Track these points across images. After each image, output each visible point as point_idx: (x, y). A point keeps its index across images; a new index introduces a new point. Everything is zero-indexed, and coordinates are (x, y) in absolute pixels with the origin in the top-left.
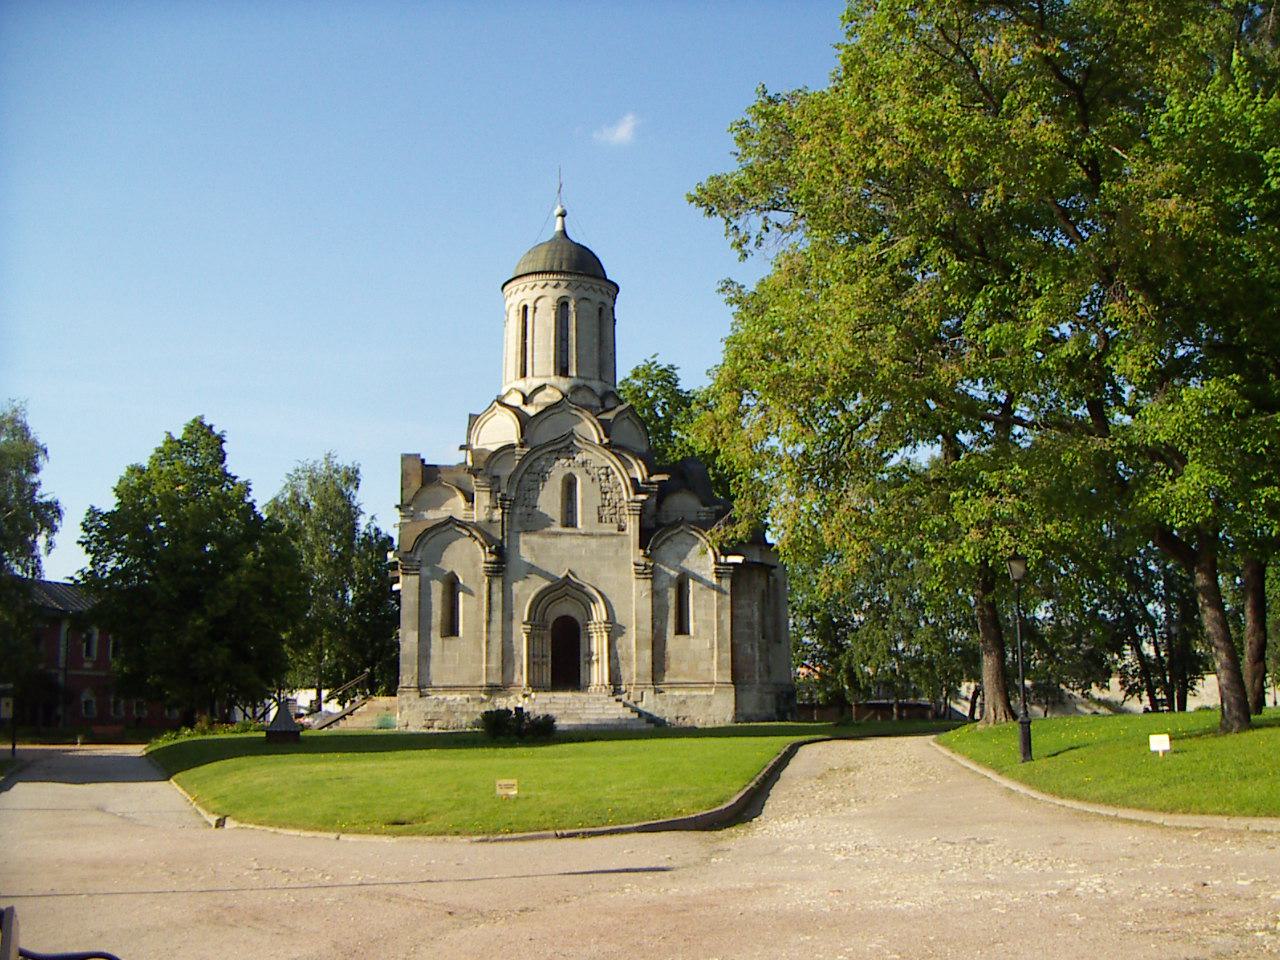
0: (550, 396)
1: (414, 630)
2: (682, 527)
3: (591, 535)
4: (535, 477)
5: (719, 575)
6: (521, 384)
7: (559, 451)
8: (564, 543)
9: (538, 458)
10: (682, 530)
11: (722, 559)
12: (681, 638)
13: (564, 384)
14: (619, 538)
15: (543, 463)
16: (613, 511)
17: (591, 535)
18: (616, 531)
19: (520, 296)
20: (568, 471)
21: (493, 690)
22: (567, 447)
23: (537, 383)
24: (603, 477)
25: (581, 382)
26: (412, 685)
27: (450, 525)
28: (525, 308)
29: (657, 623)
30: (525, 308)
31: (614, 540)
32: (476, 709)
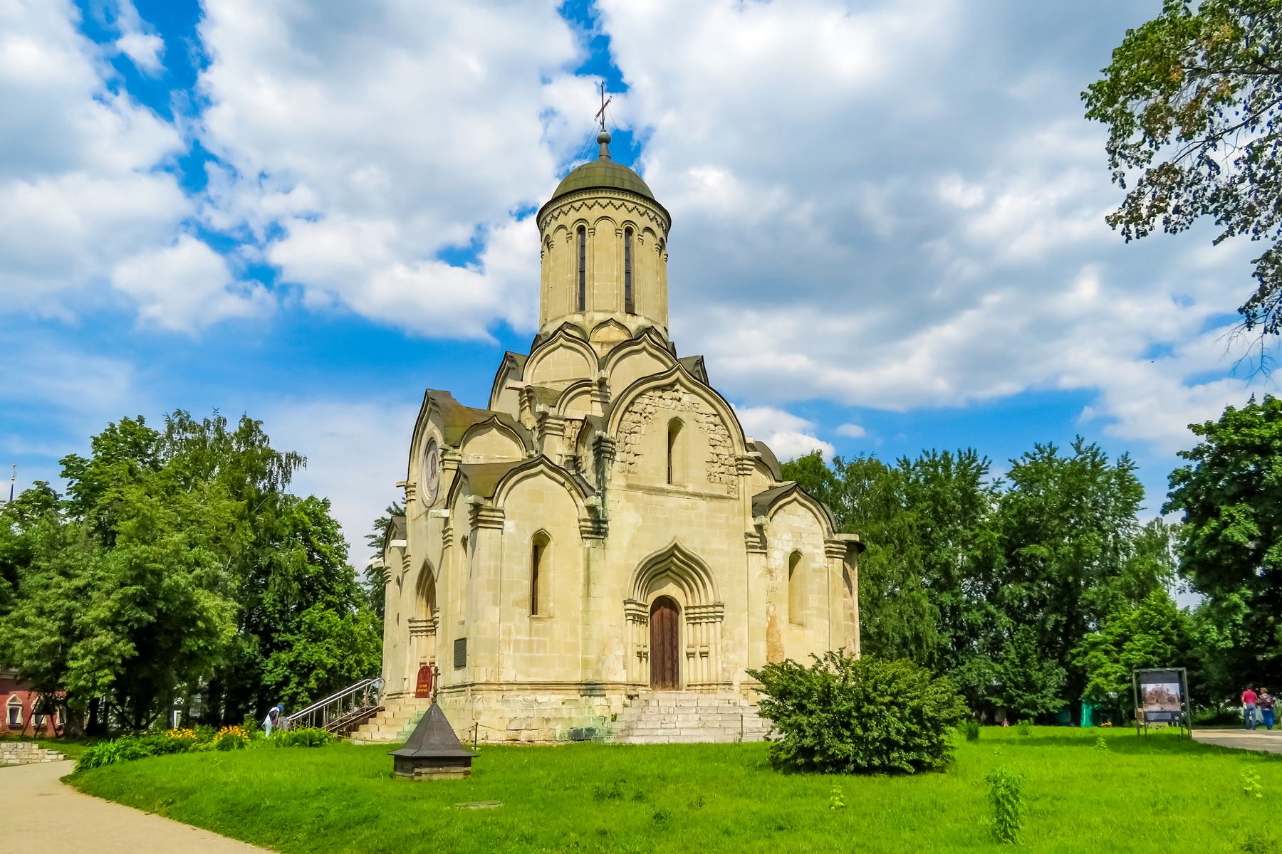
0: (618, 335)
1: (495, 604)
2: (795, 495)
3: (699, 495)
4: (637, 417)
5: (829, 553)
6: (577, 319)
7: (663, 388)
8: (672, 502)
9: (640, 395)
10: (795, 499)
11: (836, 537)
12: (797, 631)
13: (634, 324)
14: (732, 502)
15: (647, 401)
16: (723, 469)
17: (699, 495)
18: (725, 494)
19: (573, 216)
20: (674, 414)
21: (591, 688)
22: (672, 385)
23: (601, 317)
24: (712, 427)
25: (648, 324)
26: (492, 681)
27: (542, 467)
28: (581, 230)
29: (772, 609)
30: (581, 230)
31: (725, 504)
32: (573, 715)
